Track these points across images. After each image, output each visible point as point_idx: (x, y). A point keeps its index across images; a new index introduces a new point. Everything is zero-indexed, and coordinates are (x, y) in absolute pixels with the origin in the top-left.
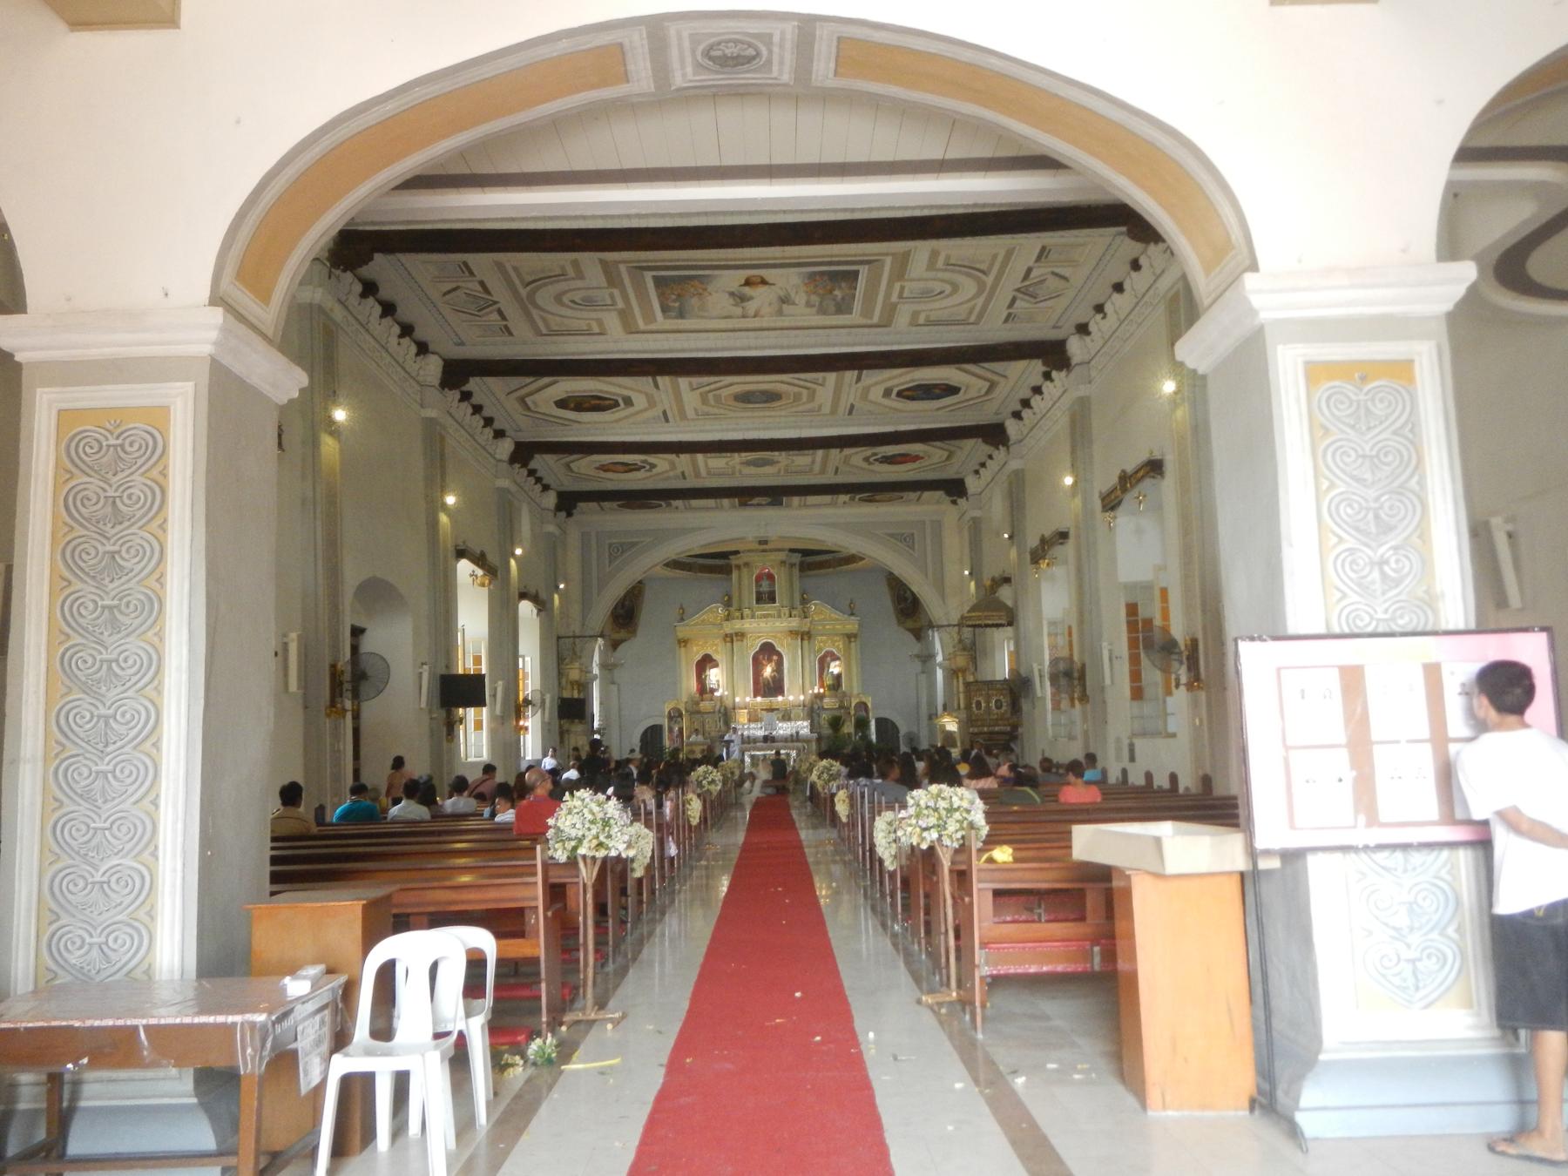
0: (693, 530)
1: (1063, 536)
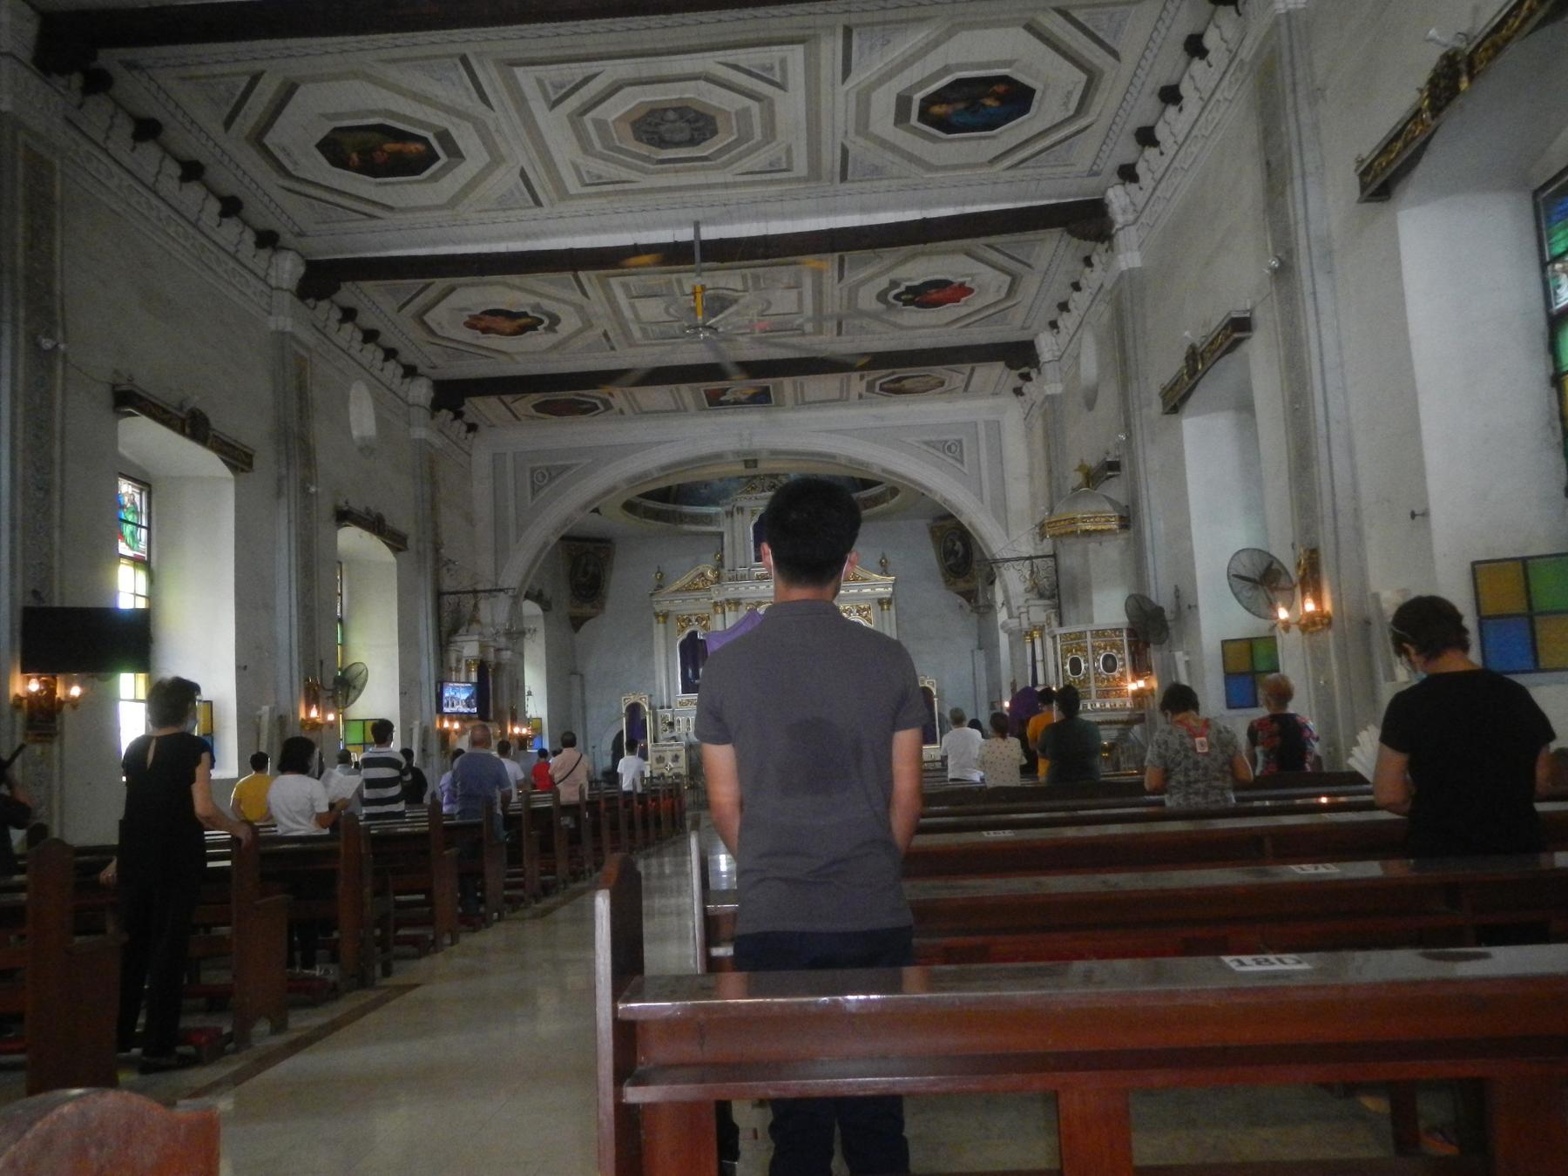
1: (1240, 326)
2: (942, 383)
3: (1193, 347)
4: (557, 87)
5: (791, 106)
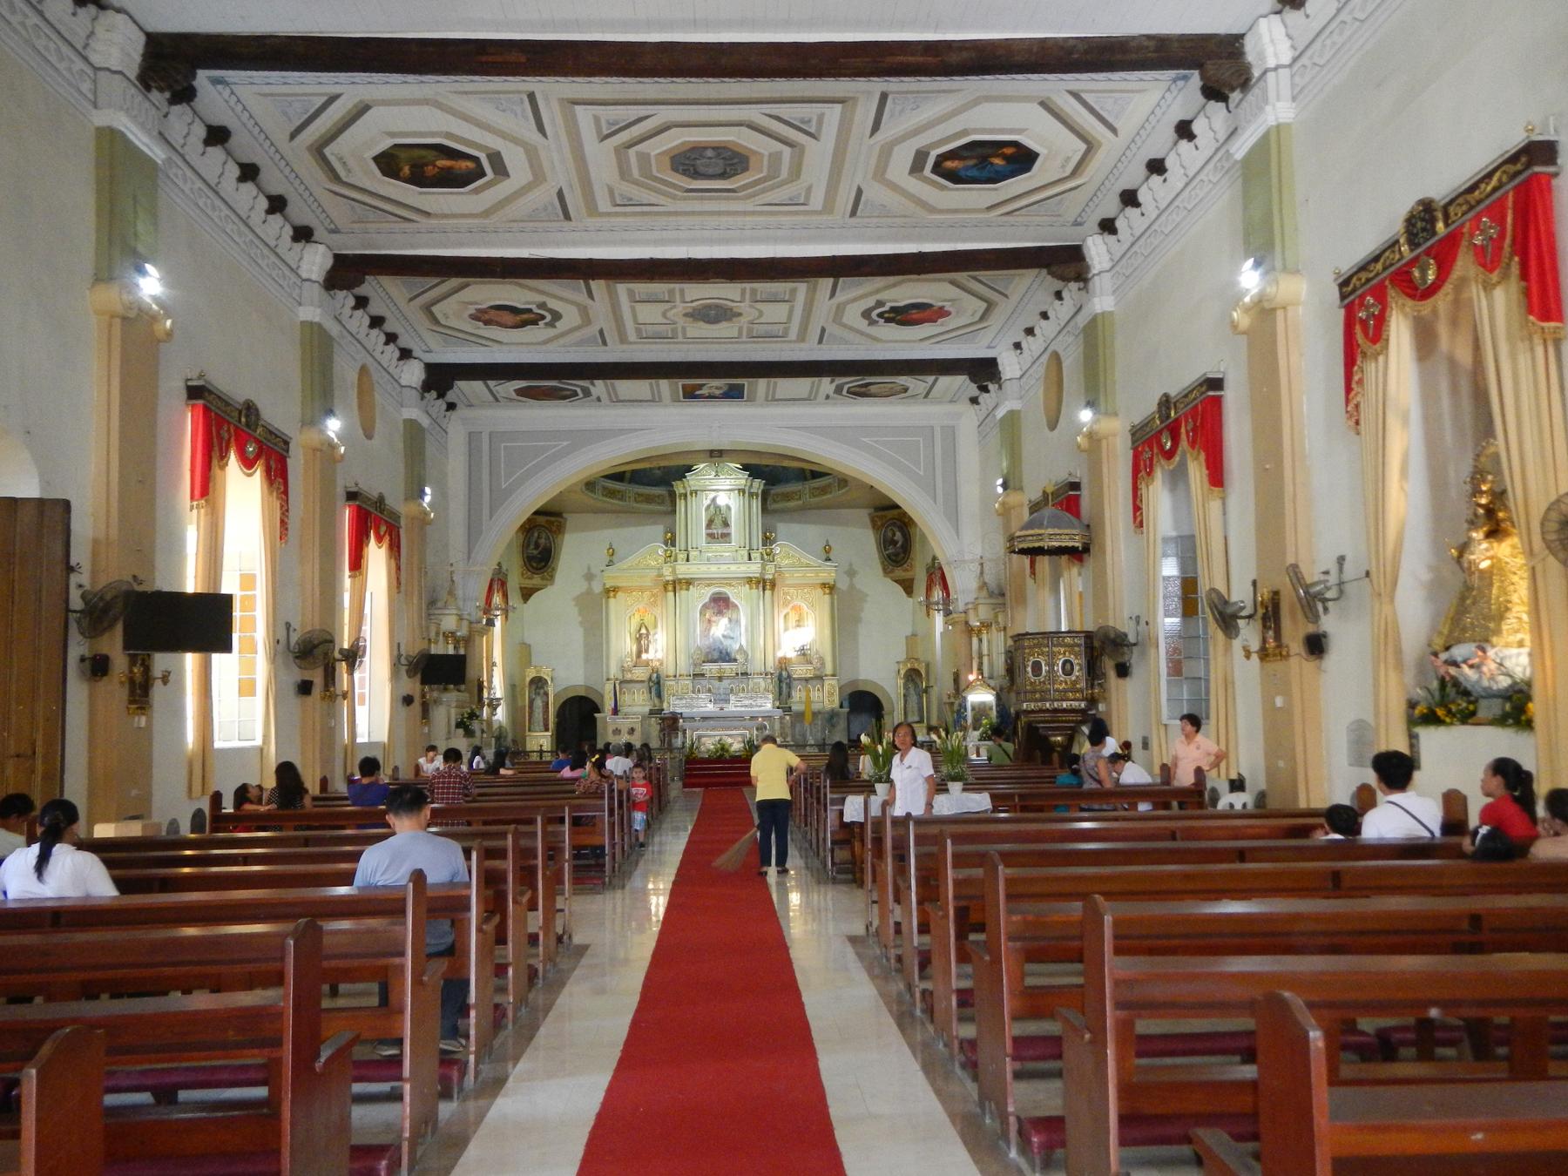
0: (622, 431)
2: (906, 390)
3: (1166, 396)
4: (610, 124)
5: (818, 154)
